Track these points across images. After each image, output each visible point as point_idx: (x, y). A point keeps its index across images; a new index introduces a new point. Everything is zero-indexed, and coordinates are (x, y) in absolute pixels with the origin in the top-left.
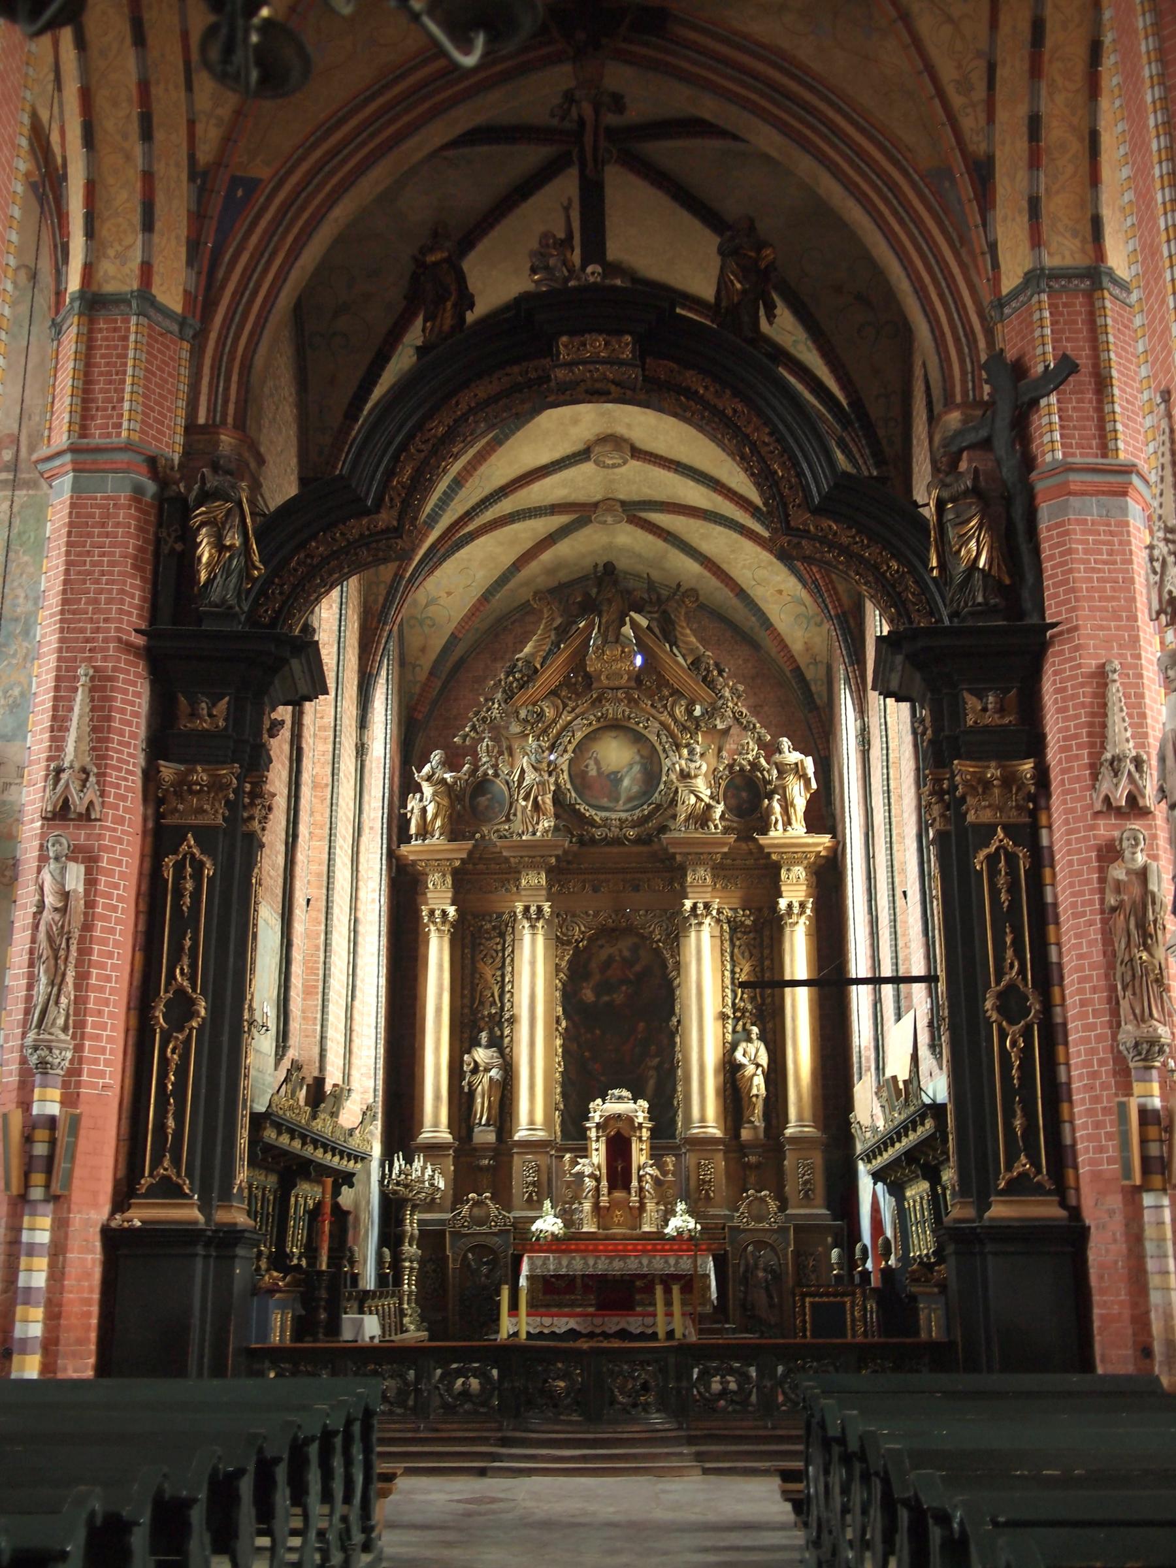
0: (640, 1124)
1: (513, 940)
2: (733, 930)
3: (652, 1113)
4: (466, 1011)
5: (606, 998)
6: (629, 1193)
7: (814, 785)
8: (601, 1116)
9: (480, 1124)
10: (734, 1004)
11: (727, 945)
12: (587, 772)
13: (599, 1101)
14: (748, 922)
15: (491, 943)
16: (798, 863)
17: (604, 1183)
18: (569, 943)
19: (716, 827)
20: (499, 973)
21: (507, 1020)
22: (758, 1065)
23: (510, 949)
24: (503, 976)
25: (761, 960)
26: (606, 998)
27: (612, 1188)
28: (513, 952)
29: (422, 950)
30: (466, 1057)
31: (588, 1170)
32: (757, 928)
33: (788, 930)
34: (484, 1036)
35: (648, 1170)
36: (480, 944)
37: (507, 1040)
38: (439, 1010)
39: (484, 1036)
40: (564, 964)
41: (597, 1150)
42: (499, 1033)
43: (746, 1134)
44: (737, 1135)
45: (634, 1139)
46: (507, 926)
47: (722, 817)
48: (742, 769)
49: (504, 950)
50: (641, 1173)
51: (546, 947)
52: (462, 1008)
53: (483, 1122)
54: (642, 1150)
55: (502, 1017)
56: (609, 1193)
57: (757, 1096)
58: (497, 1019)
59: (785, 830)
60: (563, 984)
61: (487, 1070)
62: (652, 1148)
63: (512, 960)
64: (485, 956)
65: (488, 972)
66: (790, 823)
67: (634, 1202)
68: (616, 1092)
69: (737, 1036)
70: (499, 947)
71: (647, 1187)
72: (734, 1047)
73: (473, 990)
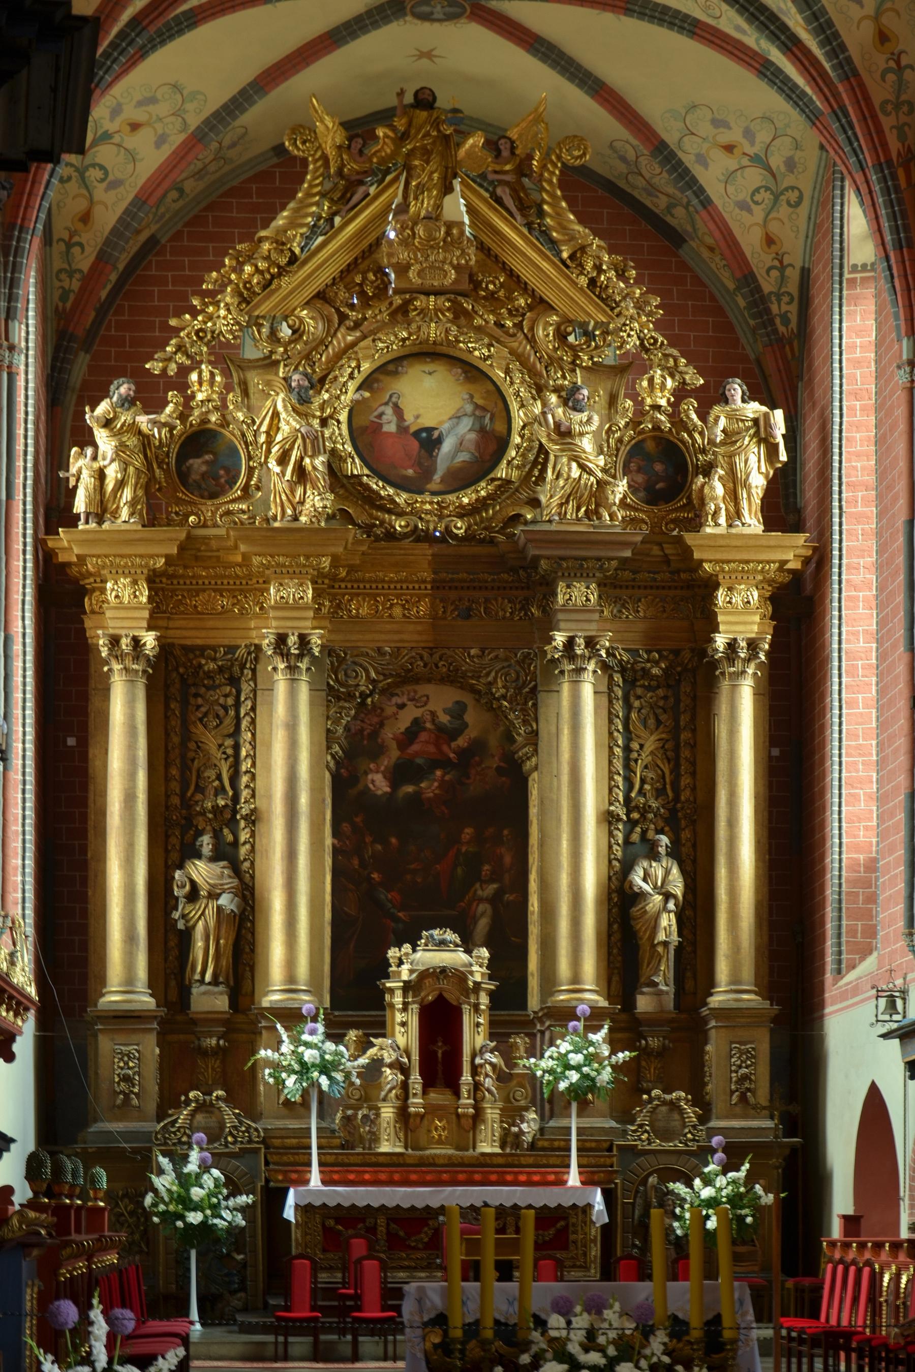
0: (477, 984)
1: (254, 691)
2: (630, 683)
3: (494, 967)
4: (176, 800)
5: (410, 789)
6: (457, 1094)
7: (783, 456)
8: (411, 971)
9: (202, 981)
10: (628, 800)
11: (619, 707)
12: (381, 425)
13: (407, 948)
14: (655, 671)
15: (213, 695)
16: (744, 576)
17: (416, 1078)
18: (350, 696)
19: (612, 516)
20: (229, 742)
21: (246, 818)
22: (667, 896)
23: (249, 704)
24: (237, 748)
25: (675, 732)
26: (410, 789)
27: (428, 1085)
28: (253, 709)
29: (95, 702)
30: (178, 874)
31: (389, 1057)
32: (670, 680)
33: (725, 684)
34: (206, 843)
35: (488, 1056)
36: (196, 695)
37: (243, 850)
38: (129, 798)
39: (206, 843)
40: (340, 730)
41: (403, 1024)
42: (230, 838)
43: (644, 1003)
44: (628, 1004)
45: (466, 1008)
46: (243, 667)
47: (623, 504)
48: (657, 428)
49: (237, 705)
50: (478, 1061)
51: (312, 703)
52: (168, 796)
53: (208, 977)
54: (478, 1025)
55: (235, 812)
56: (425, 1092)
57: (665, 944)
58: (227, 815)
59: (730, 526)
60: (337, 763)
61: (213, 896)
62: (492, 1023)
63: (253, 722)
64: (206, 714)
65: (211, 741)
66: (739, 514)
67: (466, 1106)
68: (436, 933)
69: (631, 849)
70: (230, 701)
71: (488, 1082)
72: (627, 867)
73: (185, 767)
